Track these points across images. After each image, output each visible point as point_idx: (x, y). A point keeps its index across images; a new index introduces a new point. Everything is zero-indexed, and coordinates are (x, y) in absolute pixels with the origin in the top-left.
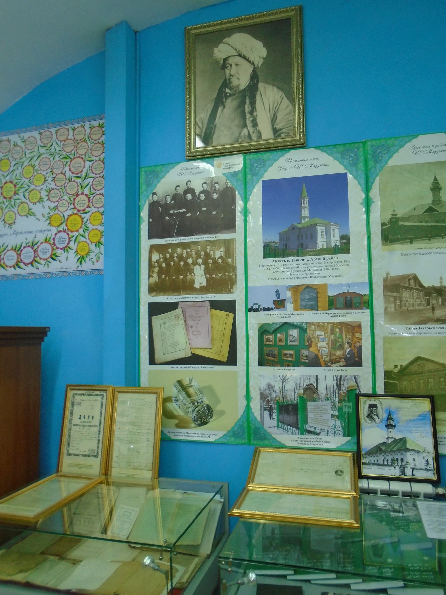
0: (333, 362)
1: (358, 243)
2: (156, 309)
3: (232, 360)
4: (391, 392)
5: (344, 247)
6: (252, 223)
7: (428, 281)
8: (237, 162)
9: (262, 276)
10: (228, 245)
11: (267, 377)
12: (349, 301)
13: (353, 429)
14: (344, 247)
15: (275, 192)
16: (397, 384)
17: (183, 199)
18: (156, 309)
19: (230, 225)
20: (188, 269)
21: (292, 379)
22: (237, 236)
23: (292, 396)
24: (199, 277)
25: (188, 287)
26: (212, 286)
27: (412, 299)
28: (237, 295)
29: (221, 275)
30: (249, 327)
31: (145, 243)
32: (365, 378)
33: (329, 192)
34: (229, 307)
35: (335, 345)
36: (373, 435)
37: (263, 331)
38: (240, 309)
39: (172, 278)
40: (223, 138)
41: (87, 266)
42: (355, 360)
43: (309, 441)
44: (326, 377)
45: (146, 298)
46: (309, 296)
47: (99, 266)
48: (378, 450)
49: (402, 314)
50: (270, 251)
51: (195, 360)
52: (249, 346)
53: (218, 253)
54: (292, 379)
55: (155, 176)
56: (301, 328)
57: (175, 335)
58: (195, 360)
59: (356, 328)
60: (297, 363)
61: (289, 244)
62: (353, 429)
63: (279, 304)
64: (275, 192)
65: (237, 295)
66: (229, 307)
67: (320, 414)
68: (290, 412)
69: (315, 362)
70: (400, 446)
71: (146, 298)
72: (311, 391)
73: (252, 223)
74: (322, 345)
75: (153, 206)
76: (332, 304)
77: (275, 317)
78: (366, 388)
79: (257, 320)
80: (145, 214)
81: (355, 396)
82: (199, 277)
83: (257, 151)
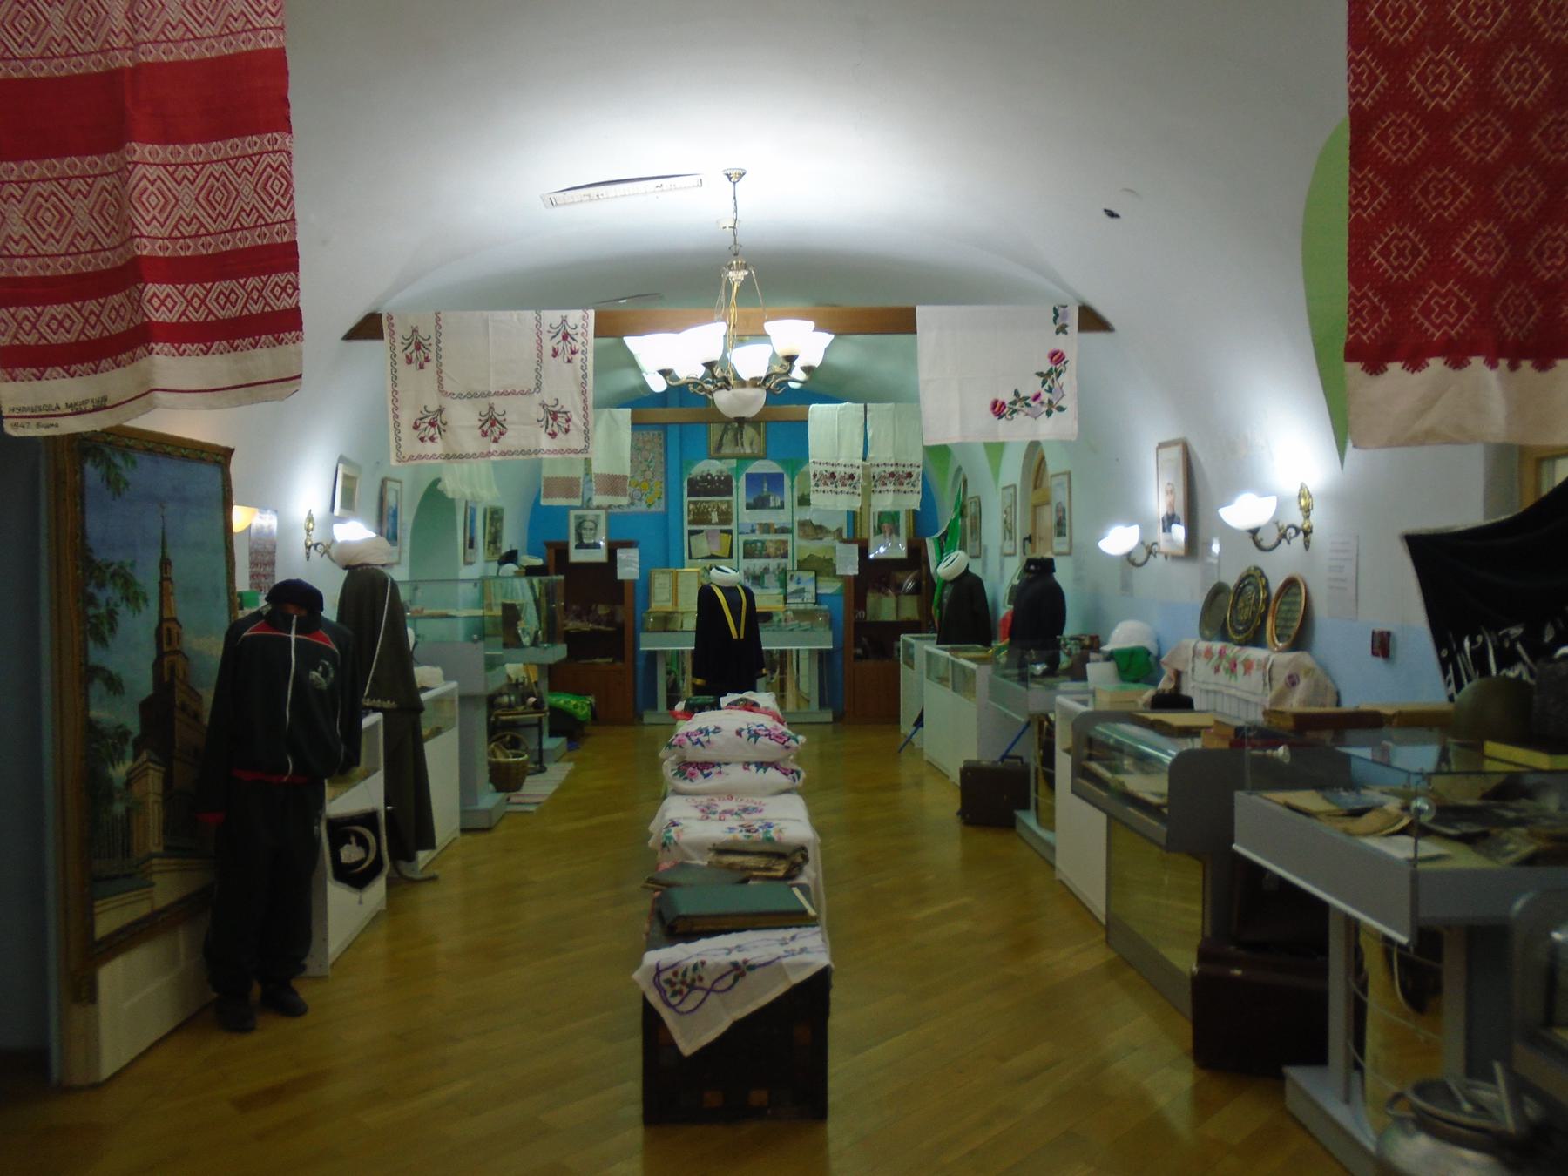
0: (776, 556)
1: (788, 505)
2: (691, 533)
3: (730, 556)
4: (800, 568)
5: (782, 506)
6: (740, 493)
7: (815, 522)
8: (734, 463)
9: (745, 517)
10: (729, 502)
11: (746, 564)
12: (783, 530)
13: (784, 585)
14: (782, 506)
15: (752, 479)
16: (803, 565)
17: (706, 478)
18: (691, 533)
19: (730, 493)
20: (709, 513)
21: (757, 564)
22: (733, 498)
23: (758, 572)
24: (715, 517)
25: (709, 522)
26: (721, 522)
27: (809, 530)
28: (733, 527)
29: (725, 517)
30: (739, 541)
31: (686, 499)
32: (789, 564)
33: (775, 481)
34: (729, 532)
35: (778, 549)
36: (792, 587)
37: (746, 543)
38: (735, 533)
39: (700, 517)
40: (726, 450)
41: (653, 509)
42: (785, 556)
43: (765, 591)
44: (773, 564)
45: (687, 528)
46: (766, 528)
47: (661, 509)
48: (795, 592)
49: (805, 536)
50: (749, 507)
51: (712, 557)
52: (738, 551)
53: (724, 507)
54: (757, 564)
55: (692, 464)
56: (763, 542)
57: (703, 545)
58: (712, 557)
59: (785, 542)
60: (760, 557)
61: (759, 503)
62: (784, 585)
63: (753, 531)
64: (752, 479)
65: (733, 527)
66: (729, 532)
67: (770, 580)
68: (758, 579)
69: (768, 557)
70: (803, 590)
71: (687, 528)
72: (766, 570)
73: (740, 493)
74: (771, 550)
75: (690, 481)
76: (777, 531)
77: (753, 537)
78: (789, 567)
79: (743, 538)
80: (685, 484)
81: (784, 571)
82: (715, 517)
83: (744, 459)
